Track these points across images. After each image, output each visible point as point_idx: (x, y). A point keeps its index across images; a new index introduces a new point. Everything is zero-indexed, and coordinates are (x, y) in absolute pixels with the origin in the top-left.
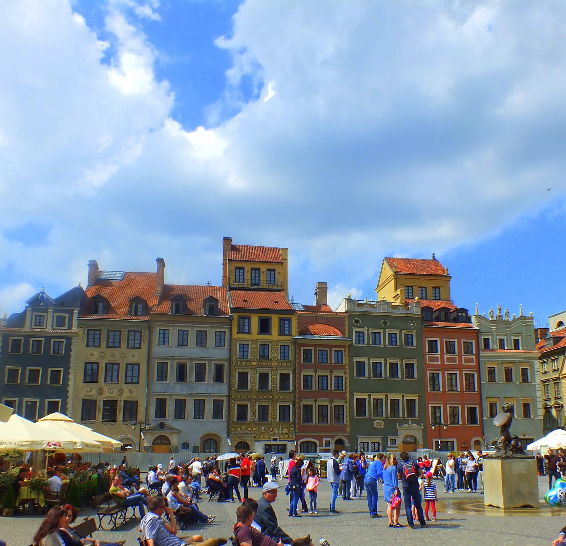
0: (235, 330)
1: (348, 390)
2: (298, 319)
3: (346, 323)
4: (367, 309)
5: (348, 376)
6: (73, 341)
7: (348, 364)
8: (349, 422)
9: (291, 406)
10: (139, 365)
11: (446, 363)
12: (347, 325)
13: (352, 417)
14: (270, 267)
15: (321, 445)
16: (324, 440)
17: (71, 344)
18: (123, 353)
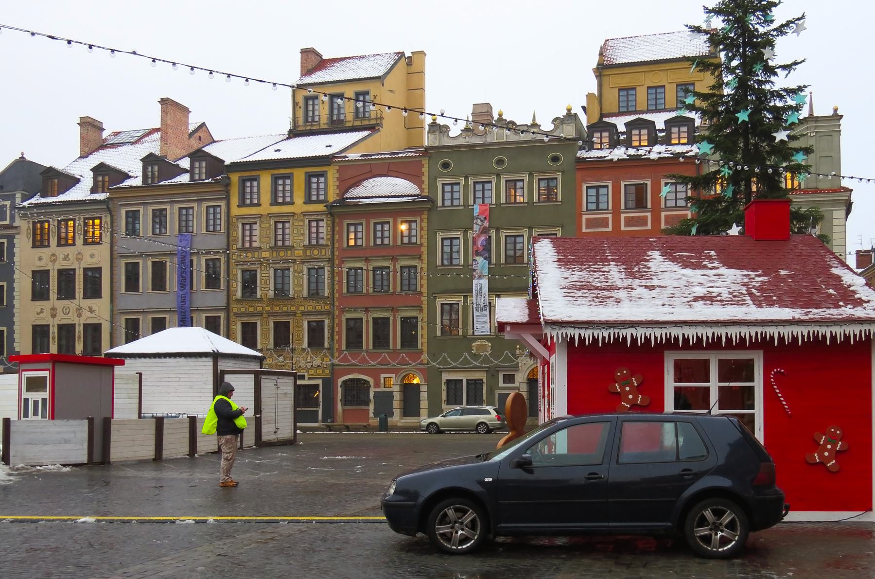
0: (235, 200)
1: (424, 291)
2: (338, 171)
3: (425, 170)
4: (467, 139)
5: (425, 265)
6: (15, 241)
7: (425, 245)
8: (425, 345)
9: (326, 322)
10: (99, 270)
11: (623, 228)
12: (426, 174)
13: (432, 337)
14: (360, 88)
15: (377, 385)
16: (382, 376)
17: (14, 246)
18: (79, 253)
